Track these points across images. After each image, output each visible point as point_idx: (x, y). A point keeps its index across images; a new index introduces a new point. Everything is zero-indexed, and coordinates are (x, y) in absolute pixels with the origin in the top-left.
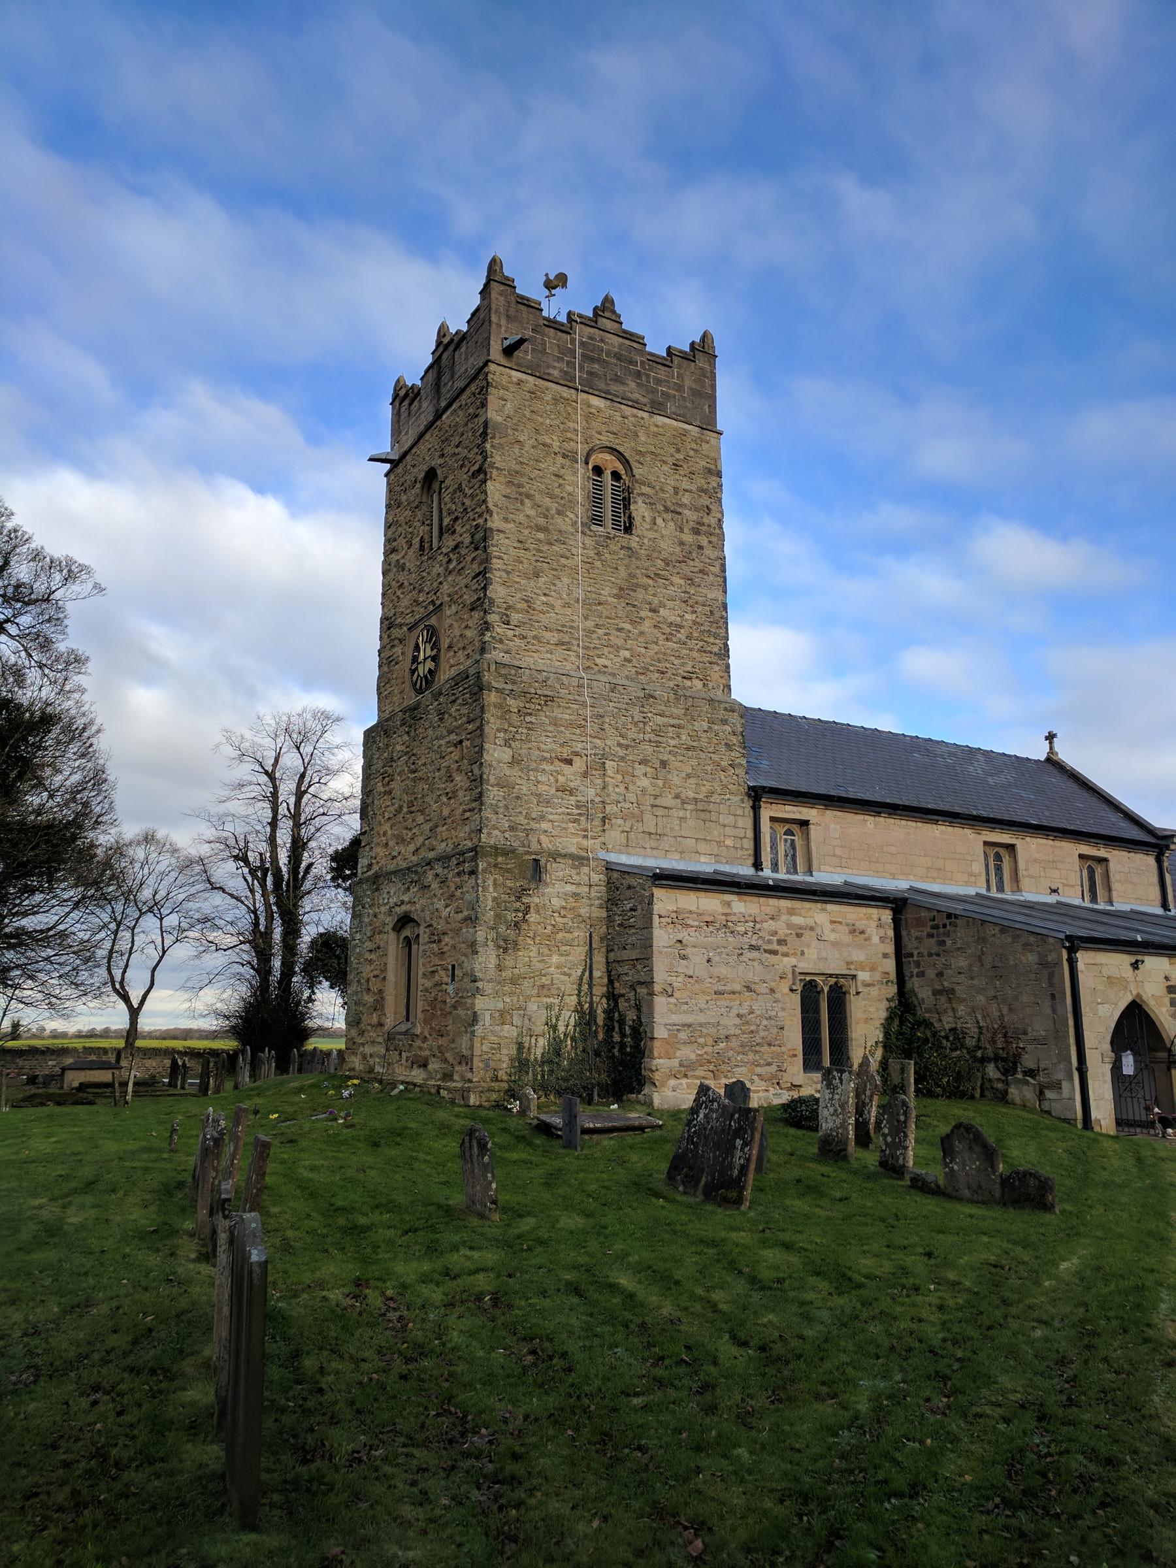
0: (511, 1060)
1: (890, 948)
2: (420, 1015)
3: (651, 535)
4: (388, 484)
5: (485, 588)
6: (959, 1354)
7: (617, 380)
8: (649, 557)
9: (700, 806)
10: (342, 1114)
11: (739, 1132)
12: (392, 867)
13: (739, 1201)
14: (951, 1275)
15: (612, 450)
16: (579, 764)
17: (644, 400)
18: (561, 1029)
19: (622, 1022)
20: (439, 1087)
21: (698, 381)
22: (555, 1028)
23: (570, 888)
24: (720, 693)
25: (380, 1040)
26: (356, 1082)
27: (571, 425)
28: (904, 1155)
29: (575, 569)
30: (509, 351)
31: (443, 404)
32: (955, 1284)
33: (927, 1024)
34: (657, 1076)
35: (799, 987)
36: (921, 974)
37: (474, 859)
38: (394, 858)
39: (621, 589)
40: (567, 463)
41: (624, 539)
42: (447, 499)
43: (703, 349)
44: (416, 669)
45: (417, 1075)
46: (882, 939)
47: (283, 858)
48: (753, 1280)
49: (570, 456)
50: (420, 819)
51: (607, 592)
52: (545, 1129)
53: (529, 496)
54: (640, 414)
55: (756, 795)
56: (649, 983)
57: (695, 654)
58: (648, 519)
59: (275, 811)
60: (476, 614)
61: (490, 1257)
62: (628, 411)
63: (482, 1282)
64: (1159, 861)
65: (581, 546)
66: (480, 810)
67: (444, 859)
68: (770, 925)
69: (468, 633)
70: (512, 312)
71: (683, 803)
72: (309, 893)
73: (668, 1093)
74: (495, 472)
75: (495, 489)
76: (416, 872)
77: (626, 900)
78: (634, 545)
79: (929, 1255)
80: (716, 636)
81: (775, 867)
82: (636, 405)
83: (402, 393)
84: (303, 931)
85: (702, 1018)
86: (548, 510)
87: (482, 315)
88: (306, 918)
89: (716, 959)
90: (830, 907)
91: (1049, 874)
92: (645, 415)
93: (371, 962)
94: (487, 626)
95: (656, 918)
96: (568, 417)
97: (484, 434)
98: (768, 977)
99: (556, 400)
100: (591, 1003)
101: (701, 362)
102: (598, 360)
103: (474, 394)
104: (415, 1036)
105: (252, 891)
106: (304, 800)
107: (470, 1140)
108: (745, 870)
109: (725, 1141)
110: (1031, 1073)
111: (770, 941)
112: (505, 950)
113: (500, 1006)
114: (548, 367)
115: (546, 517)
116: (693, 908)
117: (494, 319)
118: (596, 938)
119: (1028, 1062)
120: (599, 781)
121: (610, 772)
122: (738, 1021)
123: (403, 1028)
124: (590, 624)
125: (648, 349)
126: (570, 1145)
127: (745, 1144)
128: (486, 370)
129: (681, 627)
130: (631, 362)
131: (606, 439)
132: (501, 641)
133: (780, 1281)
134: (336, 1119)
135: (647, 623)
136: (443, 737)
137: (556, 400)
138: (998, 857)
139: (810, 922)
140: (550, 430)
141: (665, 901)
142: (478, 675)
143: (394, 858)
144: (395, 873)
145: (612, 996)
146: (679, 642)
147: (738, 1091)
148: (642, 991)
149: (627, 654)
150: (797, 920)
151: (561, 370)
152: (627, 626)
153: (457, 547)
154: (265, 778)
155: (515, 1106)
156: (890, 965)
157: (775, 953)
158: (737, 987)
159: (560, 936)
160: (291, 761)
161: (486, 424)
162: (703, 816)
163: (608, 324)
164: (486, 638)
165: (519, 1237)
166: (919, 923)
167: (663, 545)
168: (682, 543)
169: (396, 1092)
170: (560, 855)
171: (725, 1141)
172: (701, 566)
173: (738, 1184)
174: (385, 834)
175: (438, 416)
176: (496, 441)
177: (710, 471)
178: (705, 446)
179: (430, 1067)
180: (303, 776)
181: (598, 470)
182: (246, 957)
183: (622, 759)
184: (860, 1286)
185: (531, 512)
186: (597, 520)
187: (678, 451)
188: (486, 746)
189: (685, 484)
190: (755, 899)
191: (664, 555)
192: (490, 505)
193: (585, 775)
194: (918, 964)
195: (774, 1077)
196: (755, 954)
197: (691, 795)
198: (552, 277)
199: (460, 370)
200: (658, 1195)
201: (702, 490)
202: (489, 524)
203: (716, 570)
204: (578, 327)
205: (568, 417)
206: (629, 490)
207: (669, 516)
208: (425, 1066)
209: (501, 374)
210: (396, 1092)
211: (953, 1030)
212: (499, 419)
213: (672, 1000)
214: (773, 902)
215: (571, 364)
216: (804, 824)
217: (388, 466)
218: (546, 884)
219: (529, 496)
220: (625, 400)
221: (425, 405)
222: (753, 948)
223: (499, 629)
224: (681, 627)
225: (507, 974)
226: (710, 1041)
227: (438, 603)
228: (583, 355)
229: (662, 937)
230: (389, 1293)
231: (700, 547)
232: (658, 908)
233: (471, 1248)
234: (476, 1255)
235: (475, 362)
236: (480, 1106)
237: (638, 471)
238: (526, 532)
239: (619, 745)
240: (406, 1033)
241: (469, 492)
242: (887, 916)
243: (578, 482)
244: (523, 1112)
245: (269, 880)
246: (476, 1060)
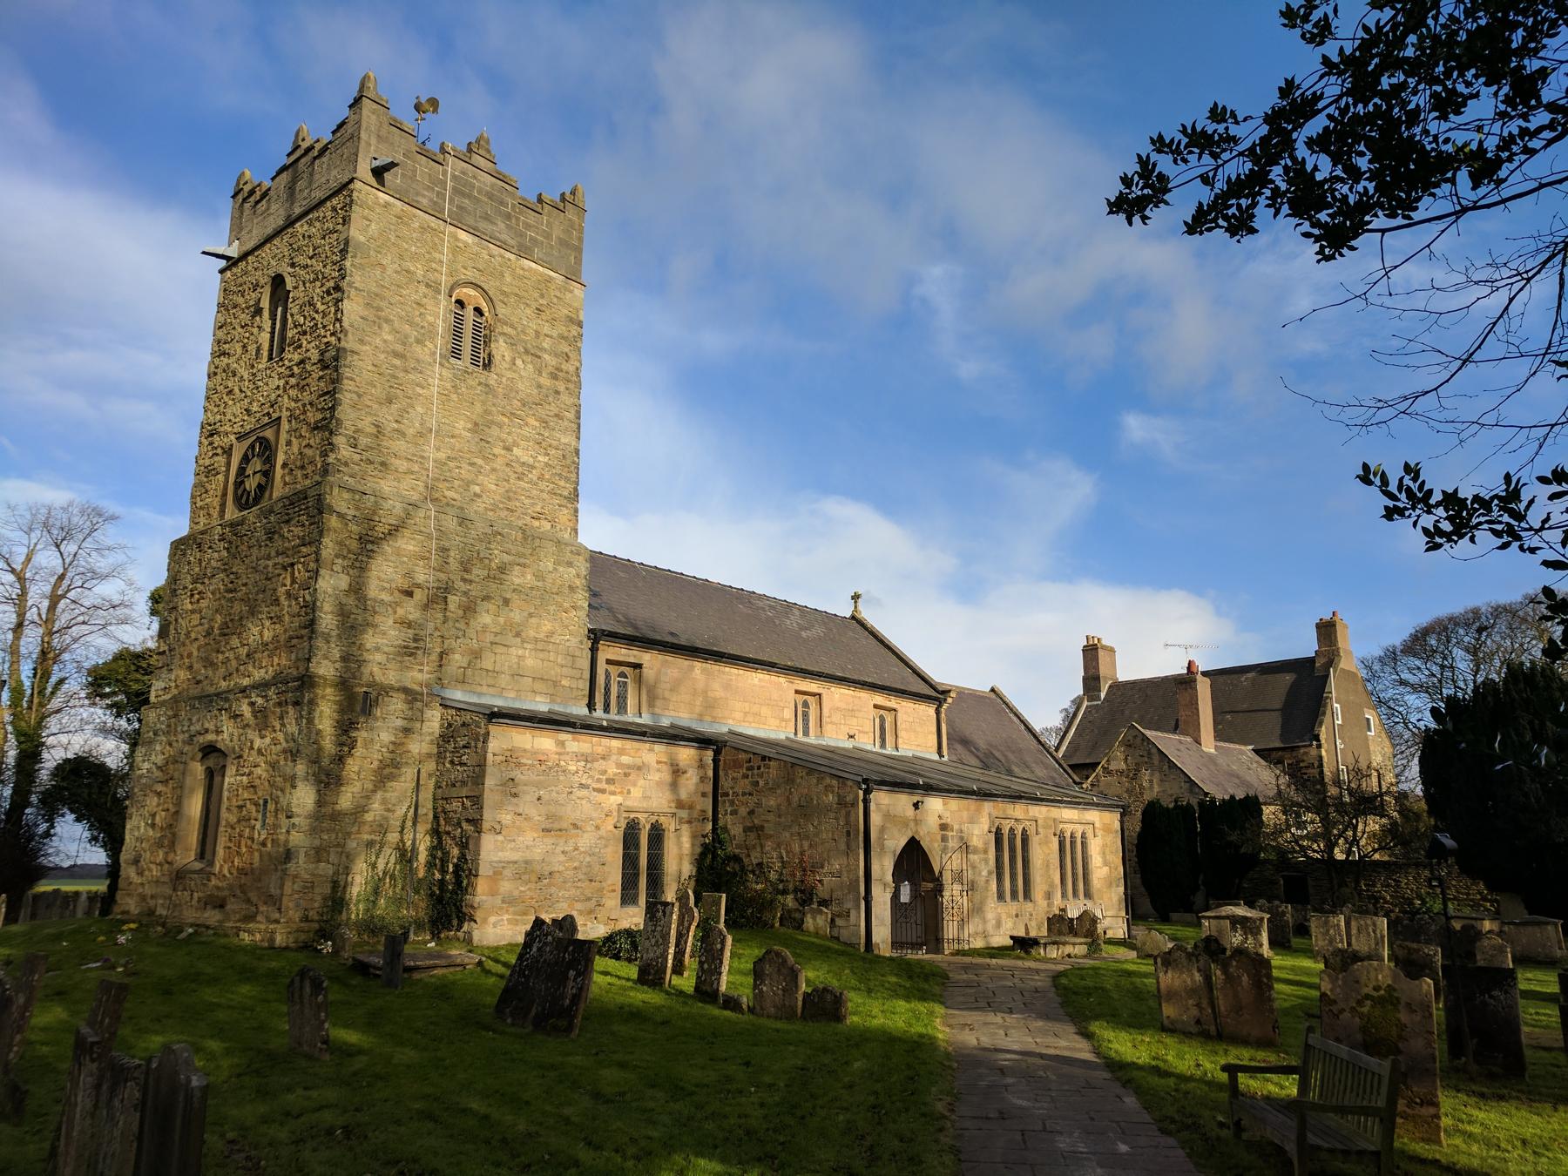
0: (325, 899)
1: (709, 788)
2: (220, 852)
3: (510, 375)
4: (223, 281)
5: (333, 408)
6: (782, 1139)
7: (487, 218)
8: (506, 396)
9: (540, 646)
10: (123, 961)
11: (572, 964)
12: (195, 691)
14: (767, 1079)
15: (477, 286)
16: (419, 595)
17: (512, 242)
18: (381, 866)
20: (239, 929)
21: (566, 231)
22: (374, 866)
24: (566, 536)
25: (166, 879)
26: (133, 926)
27: (437, 255)
28: (718, 980)
29: (429, 399)
30: (379, 173)
31: (298, 211)
32: (770, 1086)
33: (736, 858)
34: (478, 916)
36: (734, 813)
38: (198, 682)
39: (476, 424)
40: (430, 292)
41: (480, 374)
42: (295, 310)
43: (567, 201)
44: (242, 482)
45: (212, 917)
46: (702, 779)
47: (26, 670)
48: (597, 1096)
49: (433, 287)
51: (461, 425)
52: (362, 968)
53: (387, 321)
54: (508, 255)
55: (596, 637)
56: (476, 822)
57: (545, 496)
58: (507, 358)
59: (21, 615)
60: (319, 435)
61: (331, 1094)
62: (495, 250)
63: (328, 1117)
64: (938, 712)
65: (438, 377)
66: (310, 638)
67: (262, 686)
69: (309, 452)
70: (383, 133)
71: (523, 642)
74: (353, 292)
75: (352, 308)
76: (227, 700)
78: (492, 382)
79: (747, 1064)
80: (567, 479)
81: (607, 709)
82: (503, 246)
83: (247, 188)
84: (45, 755)
86: (406, 337)
87: (349, 128)
88: (50, 741)
89: (545, 797)
90: (657, 747)
91: (847, 722)
92: (512, 257)
93: (159, 794)
95: (490, 756)
96: (435, 247)
97: (344, 252)
98: (595, 815)
99: (424, 229)
100: (414, 840)
101: (571, 213)
102: (469, 196)
103: (334, 209)
106: (62, 604)
107: (302, 981)
108: (580, 710)
110: (824, 903)
111: (599, 781)
112: (327, 785)
113: (317, 842)
114: (418, 194)
115: (404, 344)
116: (528, 747)
117: (363, 135)
118: (423, 775)
119: (822, 891)
120: (440, 615)
121: (452, 607)
122: (562, 858)
123: (198, 866)
124: (442, 455)
125: (519, 193)
126: (390, 983)
127: (578, 974)
128: (351, 186)
129: (533, 467)
130: (502, 203)
131: (470, 275)
132: (346, 464)
133: (622, 1094)
134: (114, 967)
135: (500, 461)
136: (269, 557)
137: (424, 229)
138: (806, 704)
139: (638, 762)
140: (415, 257)
142: (320, 498)
143: (198, 682)
144: (200, 698)
146: (530, 482)
147: (567, 924)
149: (477, 489)
150: (625, 759)
151: (431, 200)
152: (480, 462)
153: (302, 362)
154: (11, 578)
155: (328, 947)
156: (708, 804)
157: (602, 791)
158: (565, 825)
159: (387, 771)
160: (48, 560)
161: (347, 242)
162: (541, 655)
163: (482, 162)
164: (331, 460)
165: (355, 1074)
166: (737, 764)
167: (520, 386)
168: (539, 386)
169: (183, 935)
170: (392, 688)
172: (556, 411)
173: (568, 1013)
174: (190, 655)
175: (291, 222)
176: (357, 261)
177: (571, 320)
178: (569, 295)
179: (228, 907)
180: (62, 577)
181: (460, 303)
183: (465, 593)
184: (692, 1094)
185: (389, 338)
186: (456, 353)
187: (542, 296)
188: (322, 572)
189: (546, 329)
190: (588, 738)
191: (521, 395)
192: (346, 324)
193: (426, 607)
194: (732, 803)
195: (591, 912)
196: (584, 792)
197: (532, 633)
198: (423, 100)
199: (320, 179)
200: (487, 1028)
201: (563, 338)
202: (343, 344)
203: (571, 416)
204: (451, 160)
205: (435, 247)
206: (490, 328)
207: (529, 358)
208: (222, 906)
209: (365, 191)
210: (183, 935)
211: (760, 865)
212: (362, 239)
213: (500, 838)
214: (605, 741)
215: (441, 195)
216: (638, 666)
217: (223, 263)
218: (376, 719)
219: (387, 321)
220: (491, 239)
221: (274, 207)
222: (582, 786)
223: (345, 452)
224: (533, 467)
225: (327, 810)
226: (534, 878)
227: (275, 416)
228: (454, 189)
230: (231, 1135)
231: (557, 393)
233: (306, 1089)
234: (314, 1094)
235: (337, 177)
236: (287, 948)
237: (501, 310)
238: (382, 356)
239: (464, 580)
241: (320, 307)
242: (709, 754)
243: (439, 314)
244: (336, 952)
246: (285, 900)
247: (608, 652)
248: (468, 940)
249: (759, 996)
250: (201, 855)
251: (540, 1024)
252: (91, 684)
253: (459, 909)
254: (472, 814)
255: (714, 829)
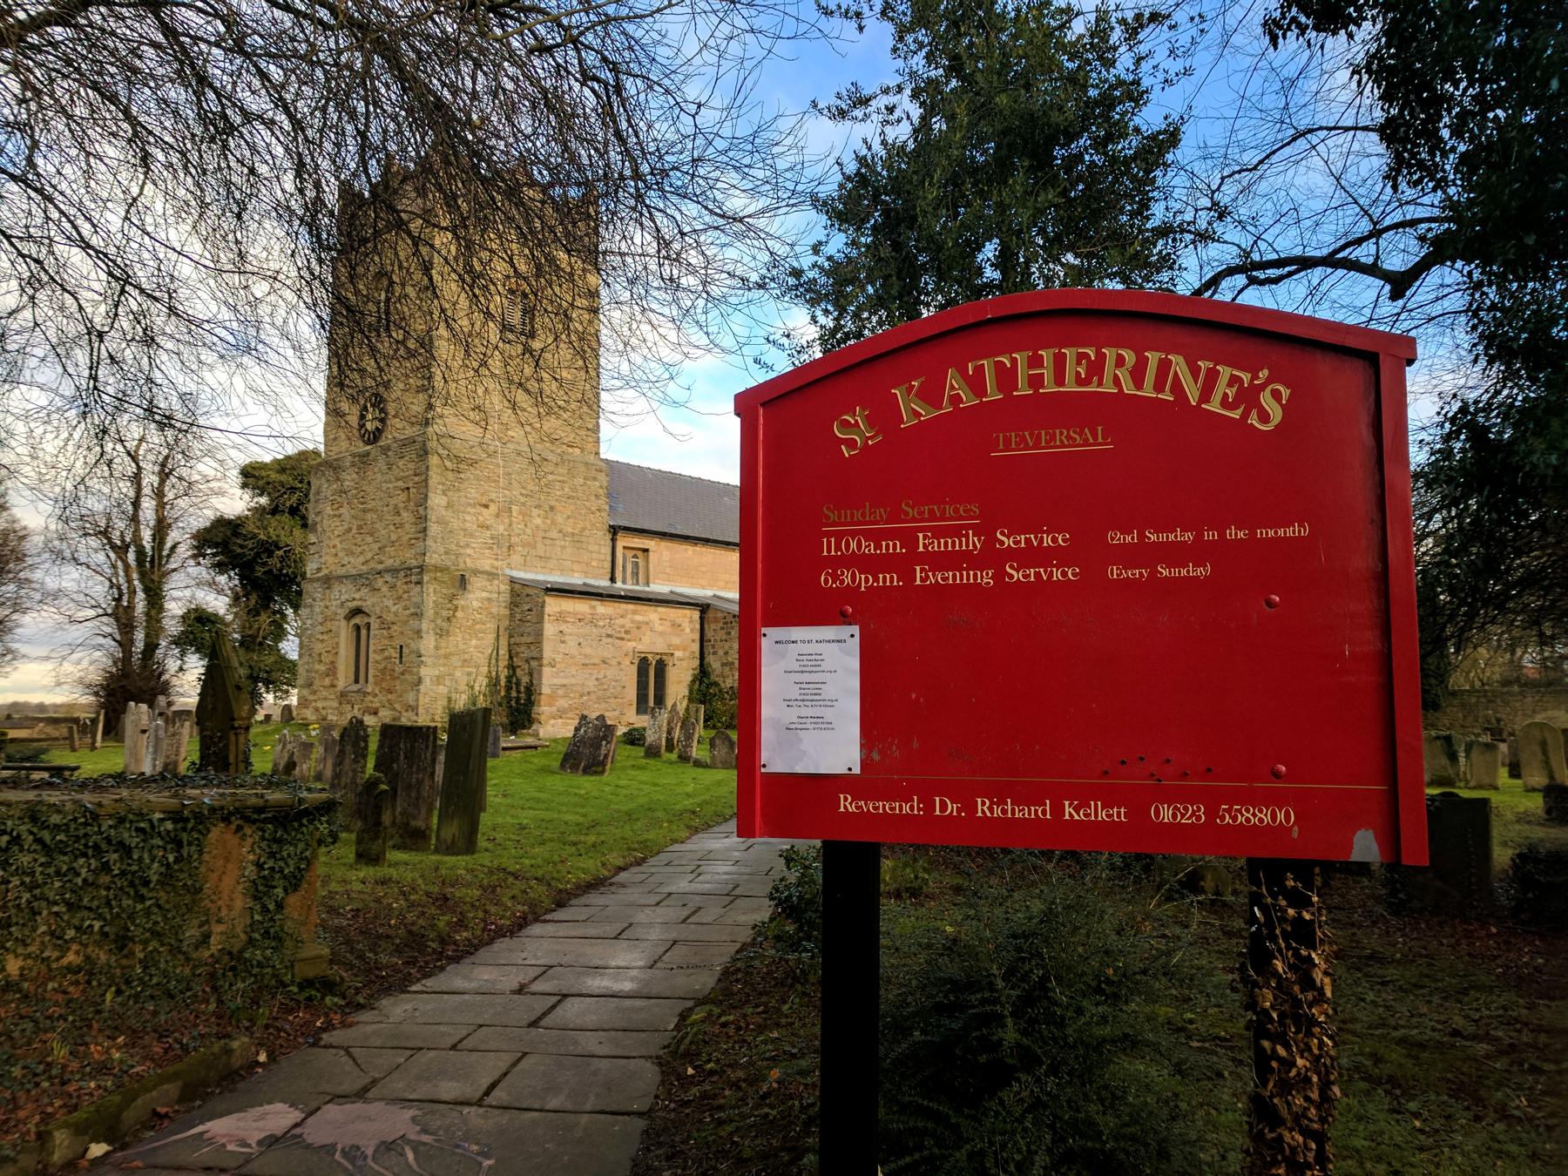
1: (697, 636)
11: (604, 738)
12: (342, 571)
13: (603, 772)
16: (493, 507)
19: (518, 684)
23: (485, 594)
33: (716, 684)
34: (542, 718)
35: (636, 661)
36: (715, 653)
37: (421, 573)
47: (146, 535)
50: (369, 539)
55: (614, 531)
56: (539, 659)
67: (394, 571)
68: (620, 621)
72: (174, 570)
73: (549, 728)
77: (525, 603)
81: (624, 582)
85: (573, 681)
90: (660, 609)
94: (430, 407)
104: (365, 694)
105: (114, 566)
108: (603, 583)
109: (595, 744)
123: (355, 687)
141: (553, 605)
145: (512, 668)
148: (534, 664)
150: (638, 618)
156: (696, 647)
158: (596, 661)
166: (716, 620)
171: (595, 744)
173: (603, 764)
182: (108, 630)
193: (497, 516)
214: (623, 606)
216: (646, 550)
222: (609, 636)
225: (442, 652)
229: (549, 629)
232: (548, 609)
240: (359, 691)
242: (696, 615)
245: (131, 556)
247: (623, 541)
248: (536, 735)
249: (713, 757)
250: (357, 681)
251: (586, 771)
252: (196, 547)
253: (529, 715)
254: (535, 654)
255: (702, 665)
